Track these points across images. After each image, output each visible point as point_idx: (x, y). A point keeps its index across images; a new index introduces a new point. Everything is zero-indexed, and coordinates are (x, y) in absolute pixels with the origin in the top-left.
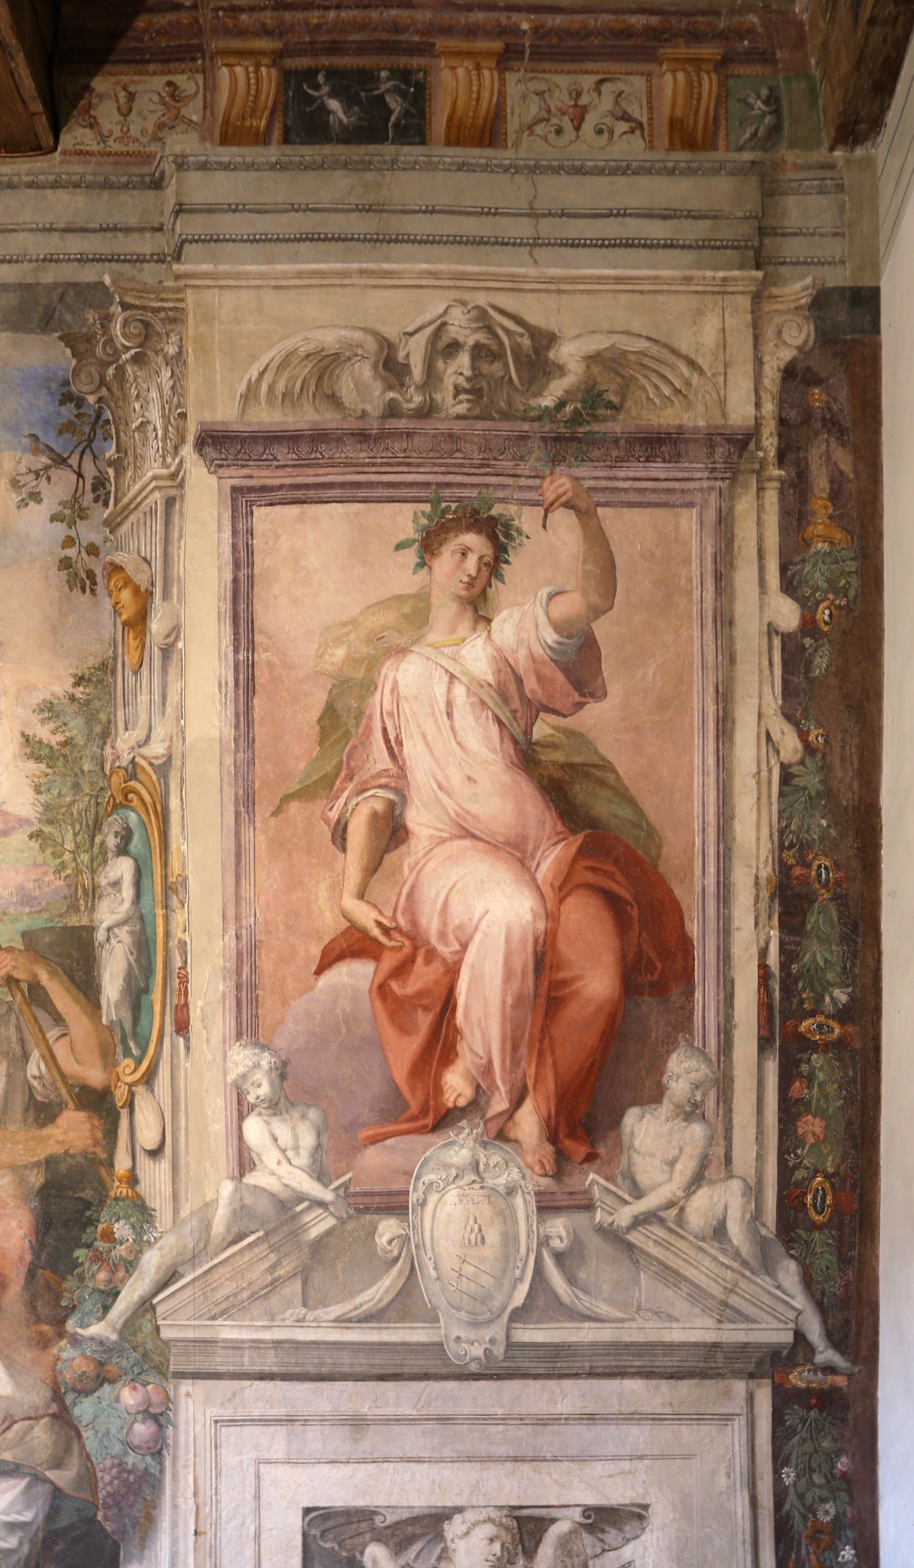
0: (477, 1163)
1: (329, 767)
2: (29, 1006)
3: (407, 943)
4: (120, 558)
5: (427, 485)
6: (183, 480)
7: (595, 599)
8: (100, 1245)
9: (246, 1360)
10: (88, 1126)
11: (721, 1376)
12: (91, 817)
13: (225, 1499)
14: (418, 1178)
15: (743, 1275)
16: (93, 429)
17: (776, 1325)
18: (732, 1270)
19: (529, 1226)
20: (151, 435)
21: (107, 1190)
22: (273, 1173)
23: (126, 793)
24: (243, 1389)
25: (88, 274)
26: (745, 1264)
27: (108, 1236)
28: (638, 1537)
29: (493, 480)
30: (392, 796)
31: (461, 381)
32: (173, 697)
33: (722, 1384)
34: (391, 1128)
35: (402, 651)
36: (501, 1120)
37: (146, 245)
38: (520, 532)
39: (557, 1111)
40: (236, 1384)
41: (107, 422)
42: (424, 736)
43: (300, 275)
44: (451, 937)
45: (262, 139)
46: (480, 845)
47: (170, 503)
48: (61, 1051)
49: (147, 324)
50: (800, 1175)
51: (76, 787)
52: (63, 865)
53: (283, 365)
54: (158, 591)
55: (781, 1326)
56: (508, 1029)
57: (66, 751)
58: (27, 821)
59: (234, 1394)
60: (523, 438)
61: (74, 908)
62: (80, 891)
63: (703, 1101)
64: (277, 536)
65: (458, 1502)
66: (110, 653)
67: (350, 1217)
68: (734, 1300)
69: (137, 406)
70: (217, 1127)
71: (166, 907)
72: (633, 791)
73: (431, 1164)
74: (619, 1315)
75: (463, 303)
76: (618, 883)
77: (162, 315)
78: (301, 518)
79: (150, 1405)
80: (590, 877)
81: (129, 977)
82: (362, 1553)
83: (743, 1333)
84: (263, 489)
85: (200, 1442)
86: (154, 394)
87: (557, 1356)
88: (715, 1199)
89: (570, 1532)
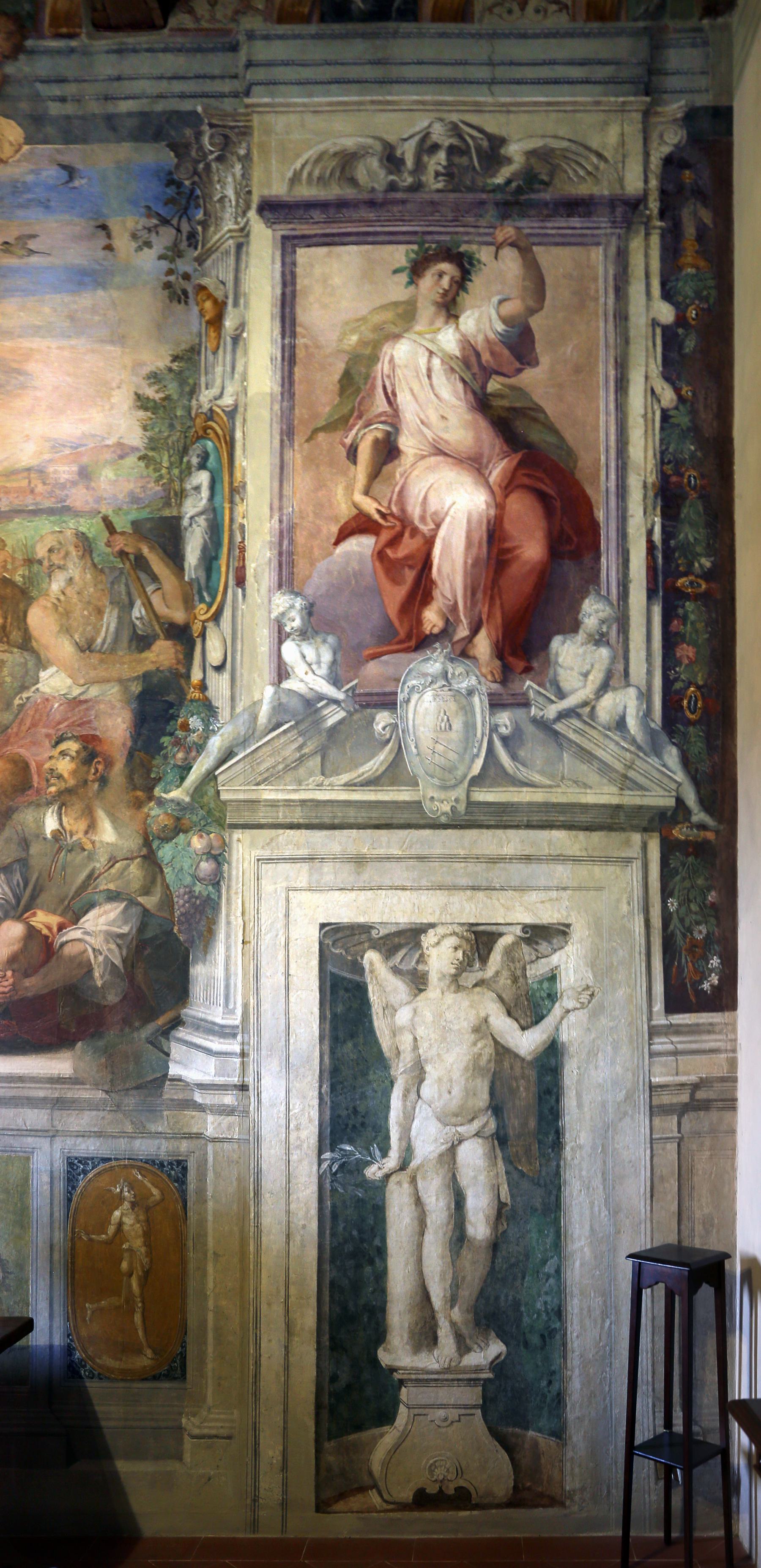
0: (447, 673)
1: (346, 410)
2: (134, 570)
3: (398, 523)
4: (205, 281)
5: (415, 233)
6: (249, 232)
7: (531, 303)
8: (180, 733)
9: (280, 814)
10: (173, 650)
11: (623, 829)
12: (181, 445)
13: (264, 917)
14: (404, 683)
15: (638, 756)
16: (188, 202)
17: (662, 793)
18: (631, 752)
19: (484, 718)
20: (228, 204)
21: (185, 695)
22: (302, 681)
23: (205, 429)
24: (278, 836)
25: (186, 106)
26: (639, 748)
27: (185, 727)
28: (562, 948)
29: (461, 229)
30: (388, 428)
31: (440, 169)
32: (239, 368)
33: (623, 835)
34: (385, 649)
35: (397, 337)
36: (463, 644)
37: (226, 86)
38: (479, 262)
39: (503, 637)
40: (273, 832)
41: (198, 197)
42: (411, 390)
43: (330, 104)
44: (429, 520)
45: (306, 19)
46: (450, 460)
47: (239, 247)
48: (156, 600)
49: (226, 137)
50: (678, 685)
51: (171, 426)
52: (161, 477)
53: (319, 158)
54: (230, 302)
55: (666, 794)
56: (469, 581)
57: (165, 403)
58: (137, 449)
59: (272, 840)
60: (482, 203)
61: (168, 504)
62: (172, 493)
63: (608, 633)
64: (312, 266)
65: (431, 920)
66: (197, 341)
67: (356, 711)
68: (631, 774)
69: (218, 187)
70: (263, 649)
71: (232, 502)
72: (558, 426)
73: (414, 673)
74: (548, 782)
75: (441, 120)
76: (546, 484)
77: (237, 130)
78: (329, 255)
79: (212, 848)
80: (526, 481)
81: (204, 549)
82: (362, 957)
83: (638, 798)
84: (303, 237)
85: (247, 875)
86: (230, 179)
87: (503, 812)
88: (618, 701)
89: (513, 943)
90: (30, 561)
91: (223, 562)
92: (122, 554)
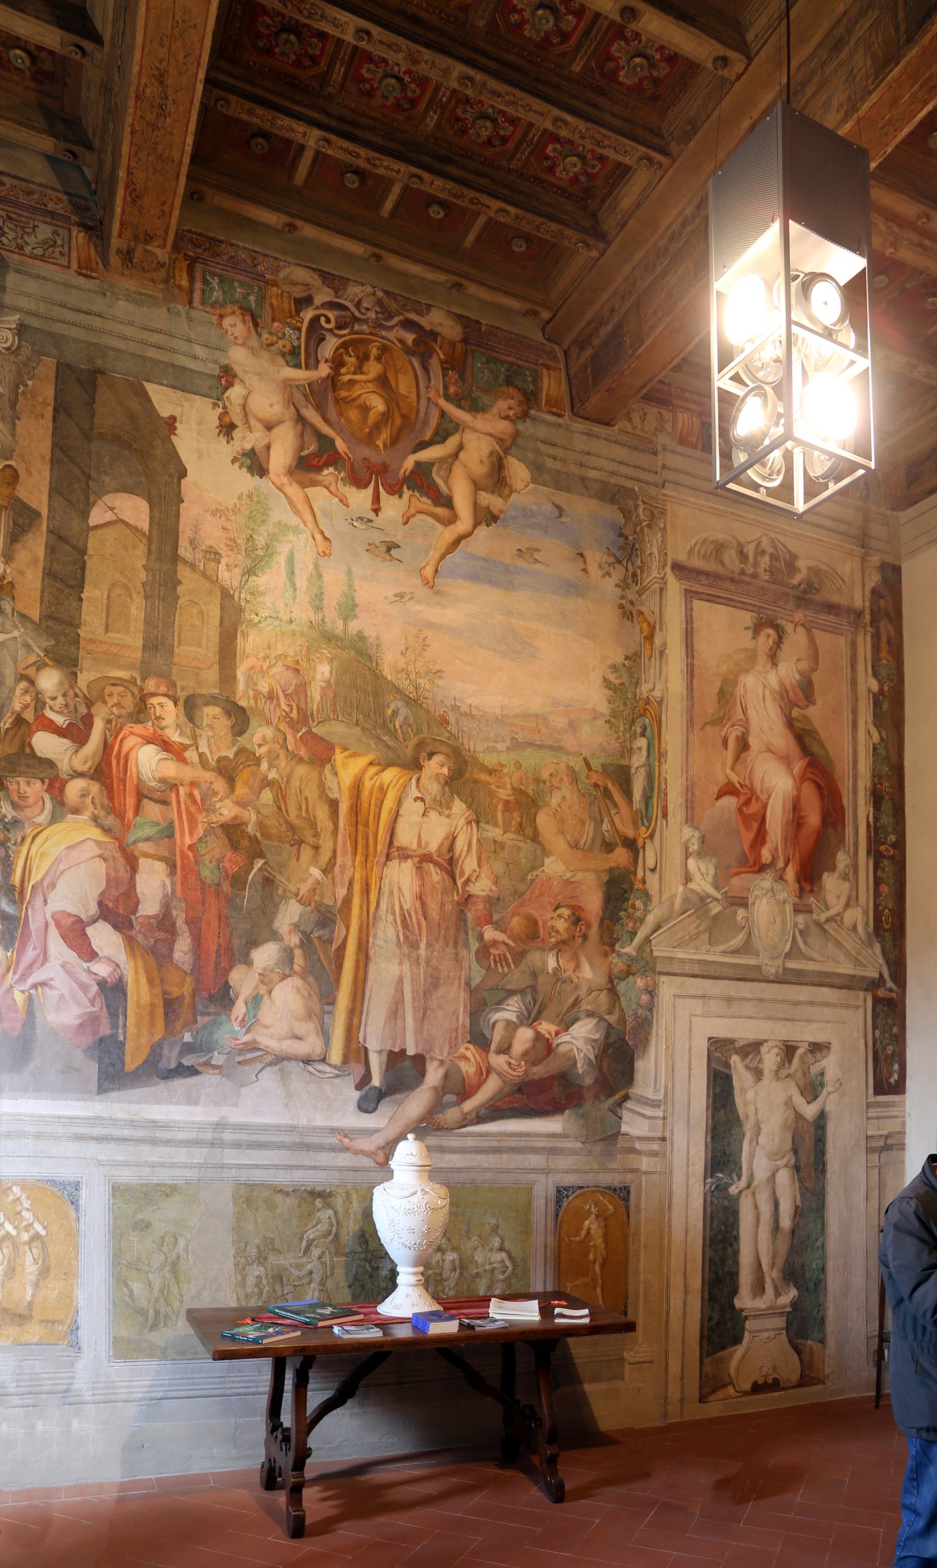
51: (625, 704)
61: (623, 756)
90: (537, 781)
91: (655, 800)
92: (596, 785)
